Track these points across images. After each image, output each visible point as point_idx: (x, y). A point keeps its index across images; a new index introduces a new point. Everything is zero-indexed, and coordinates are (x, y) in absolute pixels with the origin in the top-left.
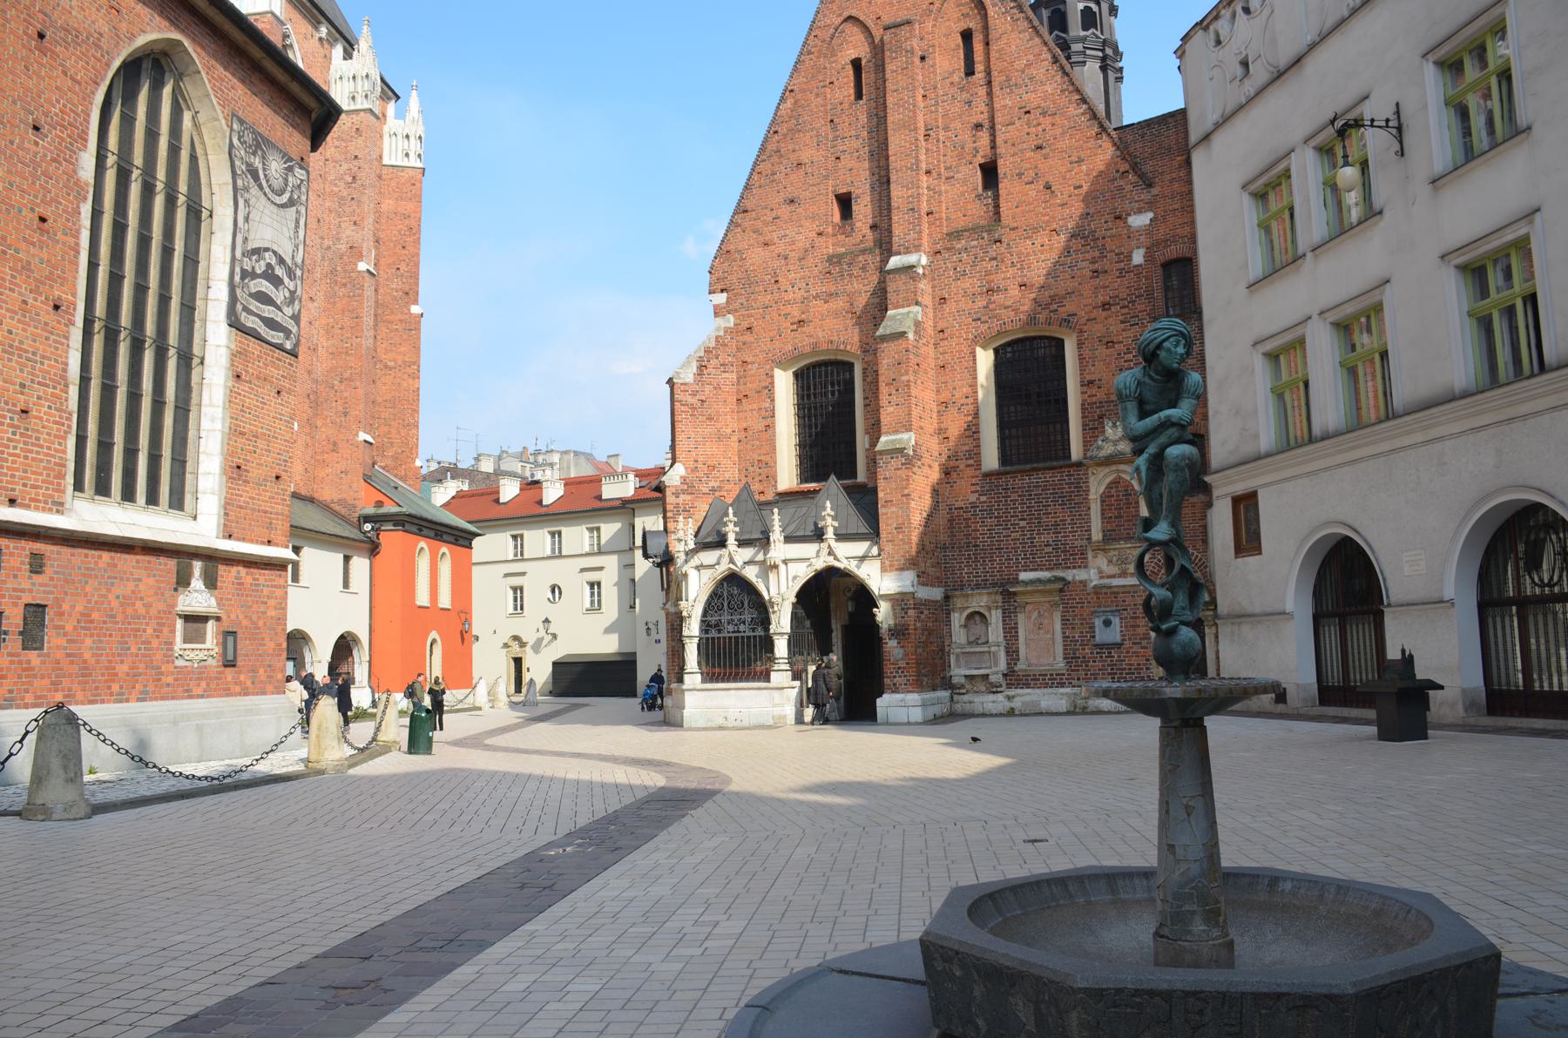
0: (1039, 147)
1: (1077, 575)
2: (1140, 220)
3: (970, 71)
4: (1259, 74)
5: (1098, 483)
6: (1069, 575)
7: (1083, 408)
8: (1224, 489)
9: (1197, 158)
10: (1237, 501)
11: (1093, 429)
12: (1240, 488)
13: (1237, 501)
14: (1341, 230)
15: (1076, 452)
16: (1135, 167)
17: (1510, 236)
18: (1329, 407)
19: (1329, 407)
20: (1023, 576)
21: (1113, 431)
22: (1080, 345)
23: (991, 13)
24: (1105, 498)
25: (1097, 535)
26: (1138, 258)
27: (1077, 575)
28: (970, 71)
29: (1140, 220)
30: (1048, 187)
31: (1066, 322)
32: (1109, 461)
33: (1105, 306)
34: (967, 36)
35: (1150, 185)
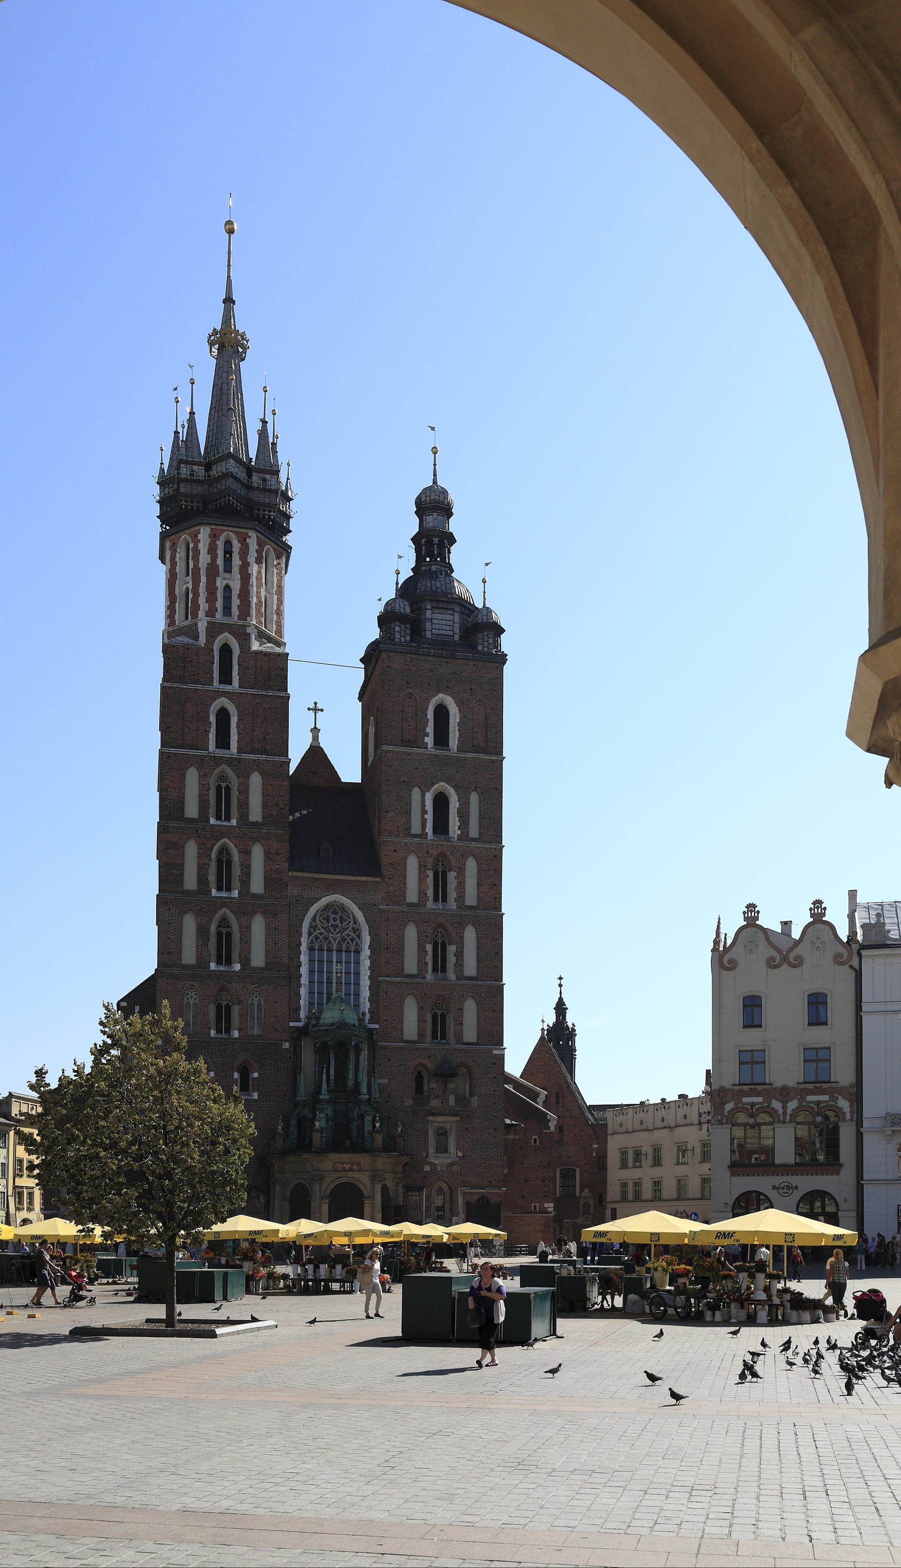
0: (574, 1126)
1: (577, 1221)
2: (595, 1146)
3: (558, 1103)
4: (624, 1129)
5: (582, 1203)
6: (574, 1220)
7: (580, 1186)
8: (610, 1206)
9: (609, 1137)
10: (612, 1209)
11: (582, 1190)
12: (613, 1206)
13: (612, 1209)
14: (635, 1167)
15: (578, 1194)
16: (595, 1134)
17: (658, 1180)
18: (631, 1196)
19: (631, 1196)
20: (564, 1220)
21: (586, 1191)
22: (580, 1172)
23: (565, 1090)
24: (583, 1205)
25: (581, 1213)
26: (594, 1154)
27: (577, 1221)
28: (558, 1103)
29: (595, 1146)
30: (575, 1135)
31: (577, 1166)
32: (585, 1197)
33: (586, 1164)
34: (558, 1094)
35: (598, 1138)
